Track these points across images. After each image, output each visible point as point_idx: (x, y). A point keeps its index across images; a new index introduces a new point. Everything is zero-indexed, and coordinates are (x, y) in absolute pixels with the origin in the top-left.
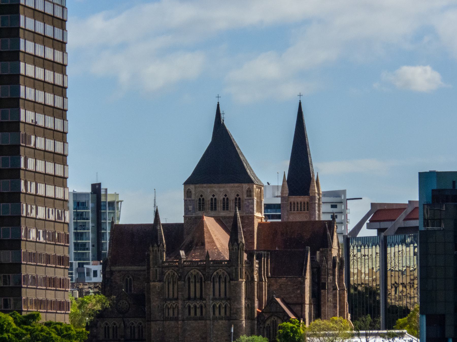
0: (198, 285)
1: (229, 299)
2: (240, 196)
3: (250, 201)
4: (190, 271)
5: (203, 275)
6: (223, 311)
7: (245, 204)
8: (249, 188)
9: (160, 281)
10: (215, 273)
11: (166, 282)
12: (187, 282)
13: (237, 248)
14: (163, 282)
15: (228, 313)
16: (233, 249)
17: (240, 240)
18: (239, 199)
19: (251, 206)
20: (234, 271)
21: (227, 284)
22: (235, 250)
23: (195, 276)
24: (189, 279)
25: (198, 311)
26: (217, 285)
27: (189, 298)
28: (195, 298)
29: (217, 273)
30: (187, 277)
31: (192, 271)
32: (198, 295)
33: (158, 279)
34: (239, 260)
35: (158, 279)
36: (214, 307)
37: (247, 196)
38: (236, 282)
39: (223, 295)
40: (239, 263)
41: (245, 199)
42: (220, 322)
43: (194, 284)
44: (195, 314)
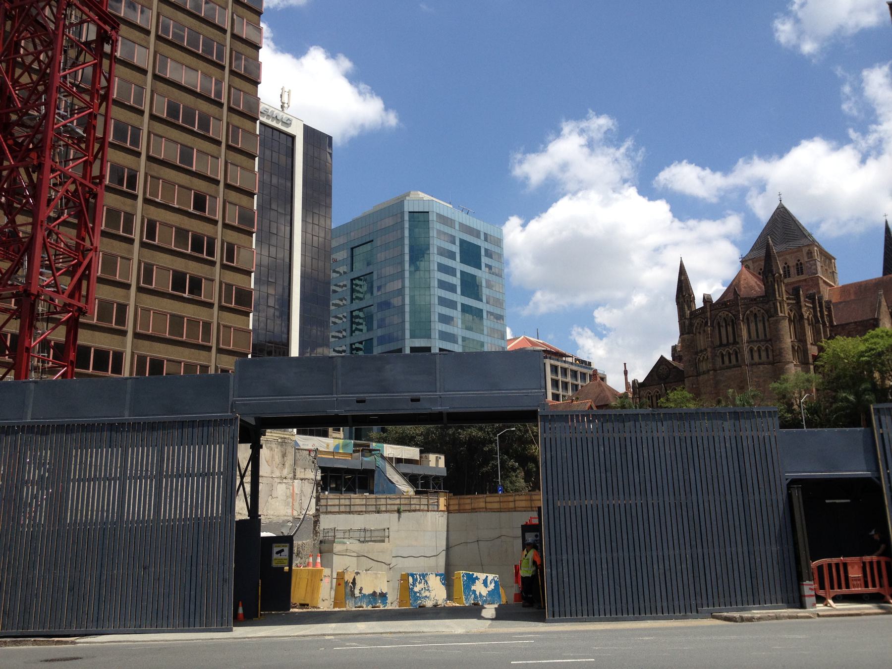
0: (730, 329)
1: (770, 340)
2: (802, 261)
3: (811, 262)
4: (717, 315)
5: (733, 315)
6: (763, 354)
7: (807, 267)
8: (809, 250)
9: (688, 333)
10: (748, 312)
11: (696, 334)
12: (717, 328)
13: (772, 279)
14: (693, 333)
15: (771, 357)
16: (768, 282)
17: (774, 269)
18: (801, 263)
19: (814, 267)
20: (772, 306)
21: (767, 324)
22: (770, 283)
23: (724, 319)
24: (719, 323)
25: (733, 358)
26: (753, 325)
27: (721, 345)
28: (728, 344)
29: (751, 312)
30: (715, 321)
31: (720, 314)
32: (731, 340)
33: (687, 331)
34: (777, 293)
35: (687, 331)
36: (751, 350)
37: (808, 258)
38: (775, 318)
39: (762, 336)
40: (777, 296)
41: (806, 262)
42: (761, 367)
43: (724, 328)
44: (730, 362)
